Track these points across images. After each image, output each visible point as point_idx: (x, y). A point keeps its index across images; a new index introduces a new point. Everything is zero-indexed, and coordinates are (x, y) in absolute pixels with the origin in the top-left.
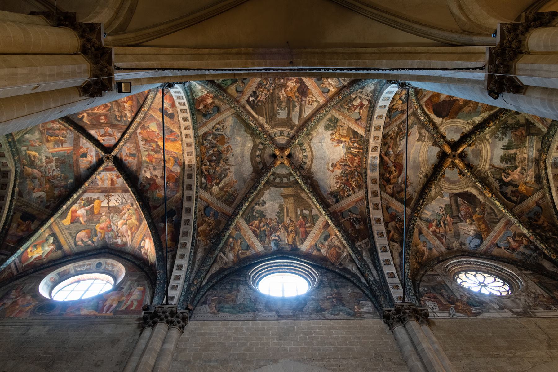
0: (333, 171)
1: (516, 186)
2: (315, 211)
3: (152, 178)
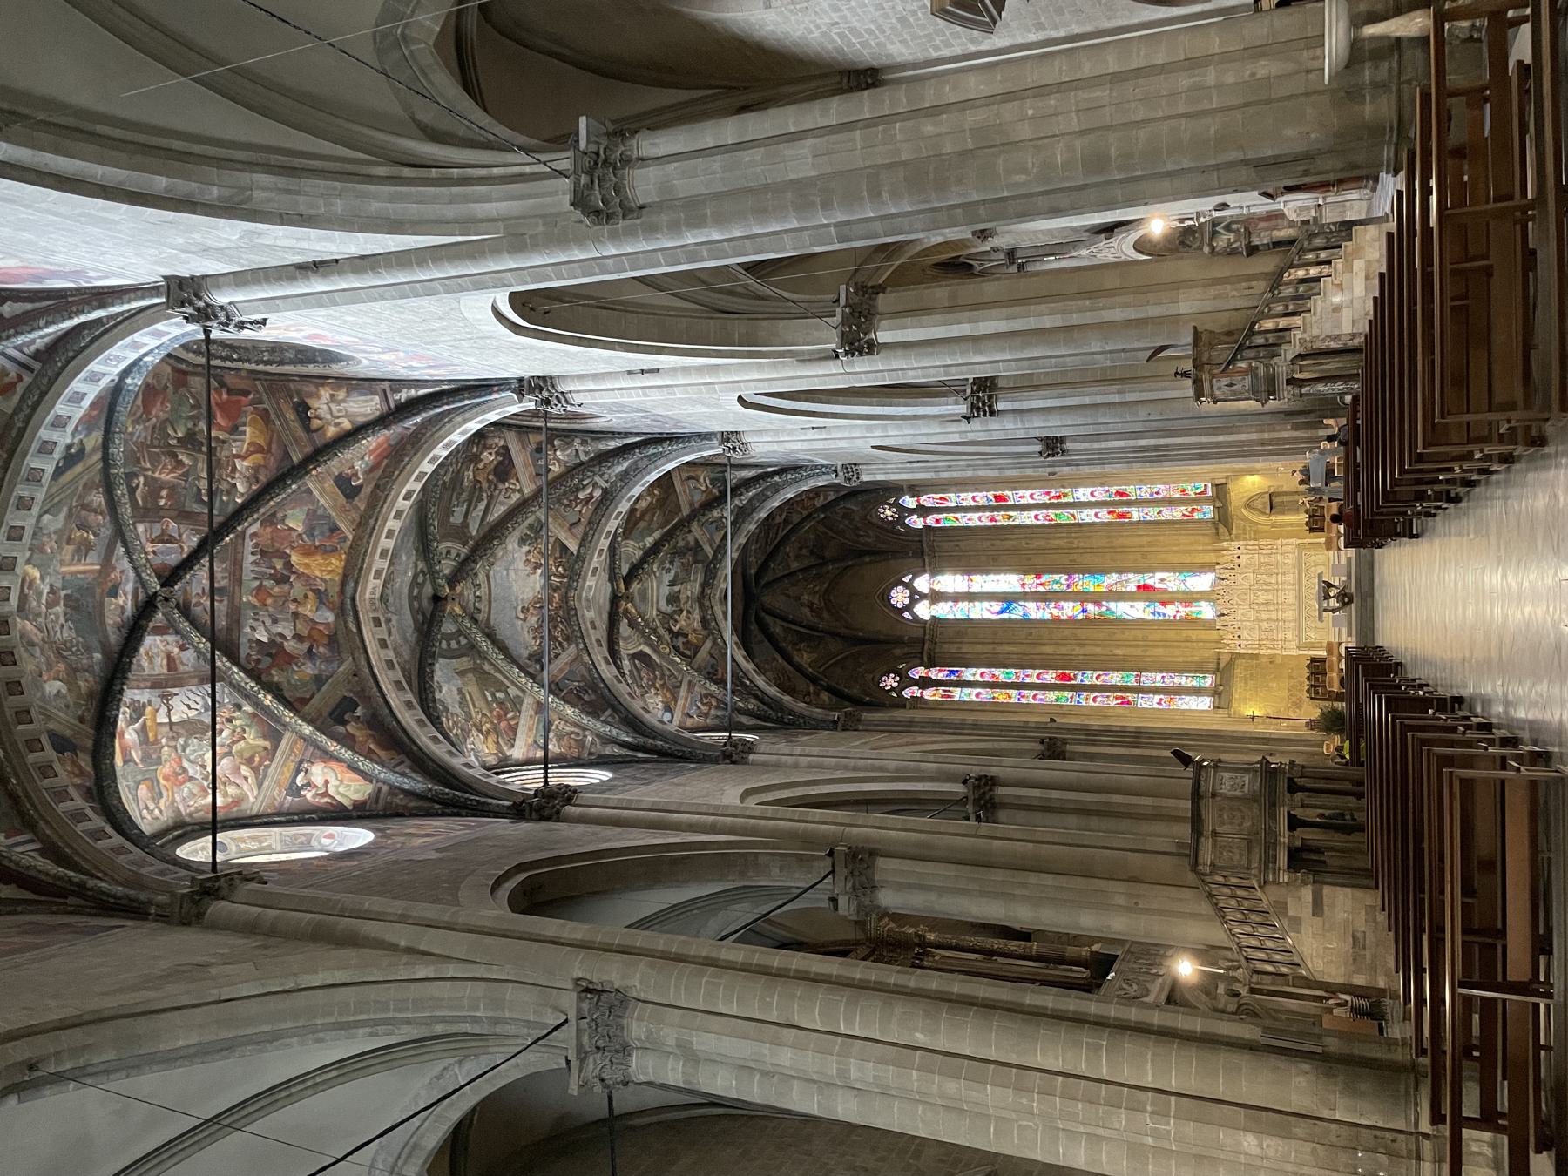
0: (525, 620)
1: (686, 636)
2: (513, 691)
3: (272, 642)
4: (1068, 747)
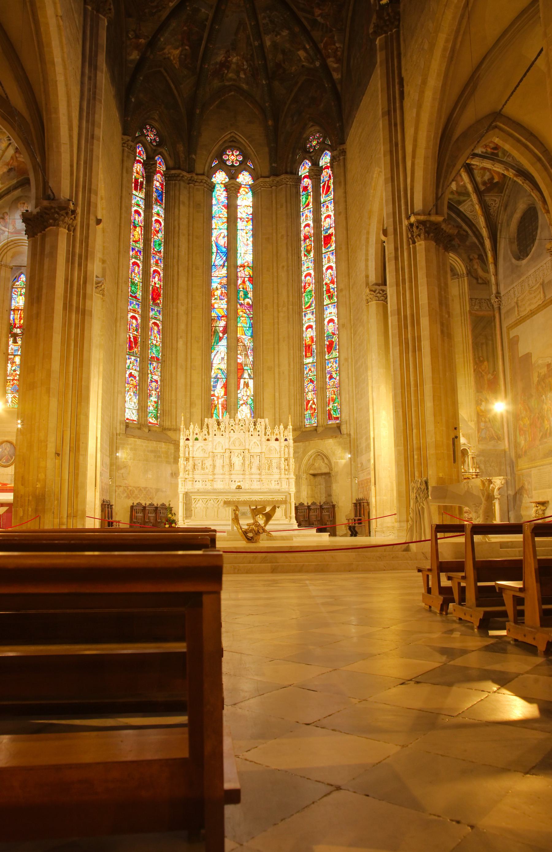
4: (63, 231)
